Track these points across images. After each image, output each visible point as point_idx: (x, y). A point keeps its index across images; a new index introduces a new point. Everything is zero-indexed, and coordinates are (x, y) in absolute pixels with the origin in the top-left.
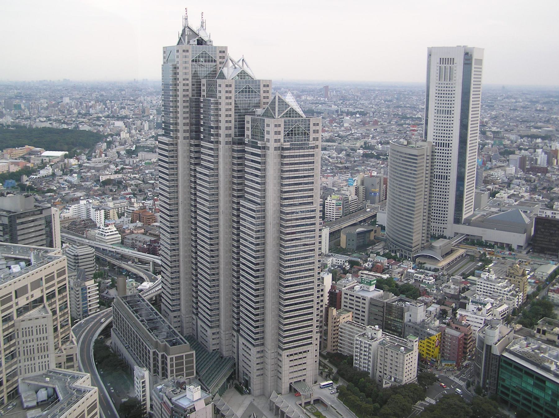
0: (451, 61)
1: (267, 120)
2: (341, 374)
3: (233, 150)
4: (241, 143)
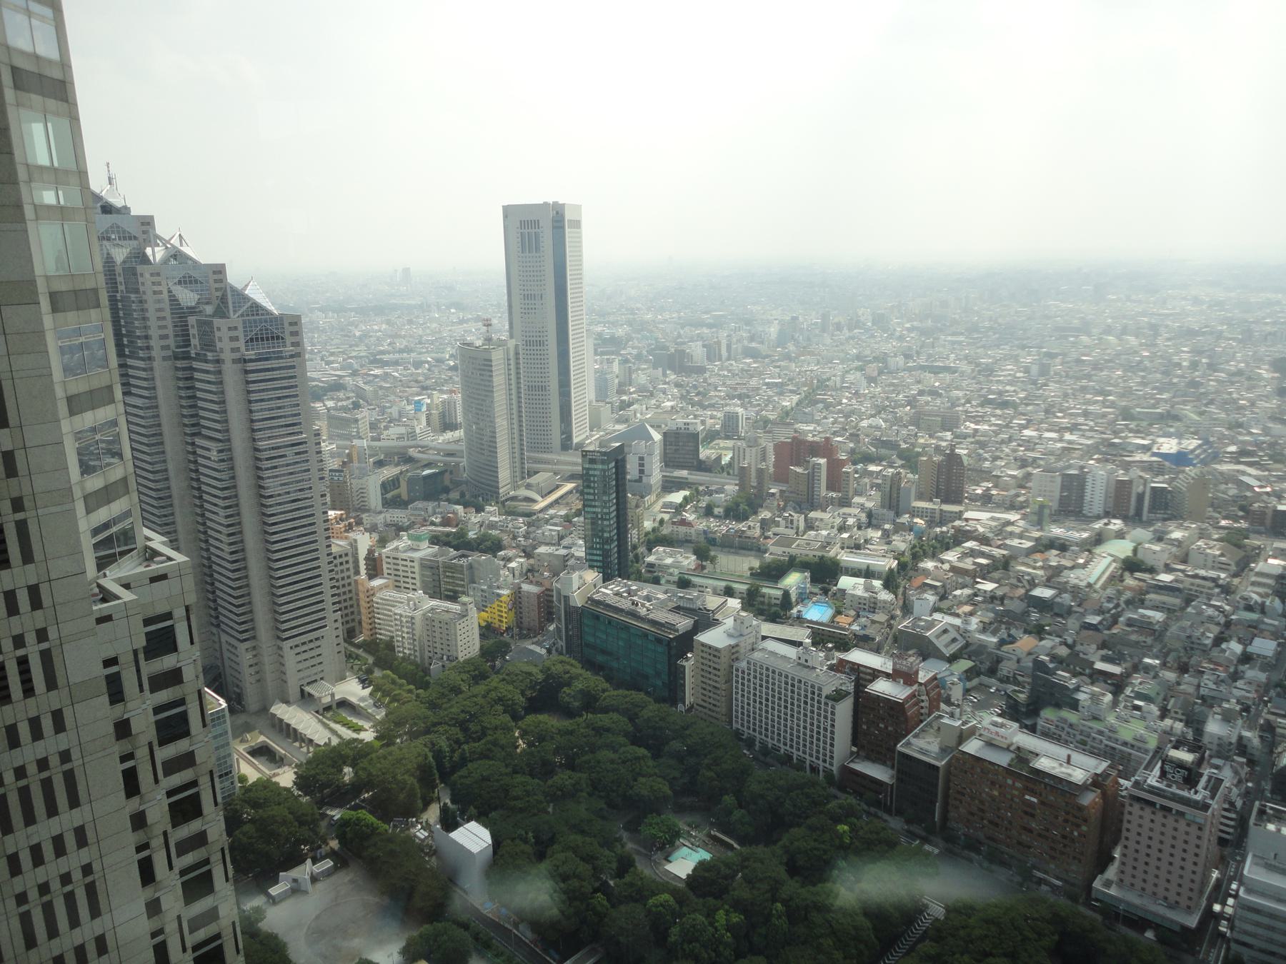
0: (536, 224)
1: (217, 322)
2: (382, 663)
3: (177, 369)
4: (186, 357)
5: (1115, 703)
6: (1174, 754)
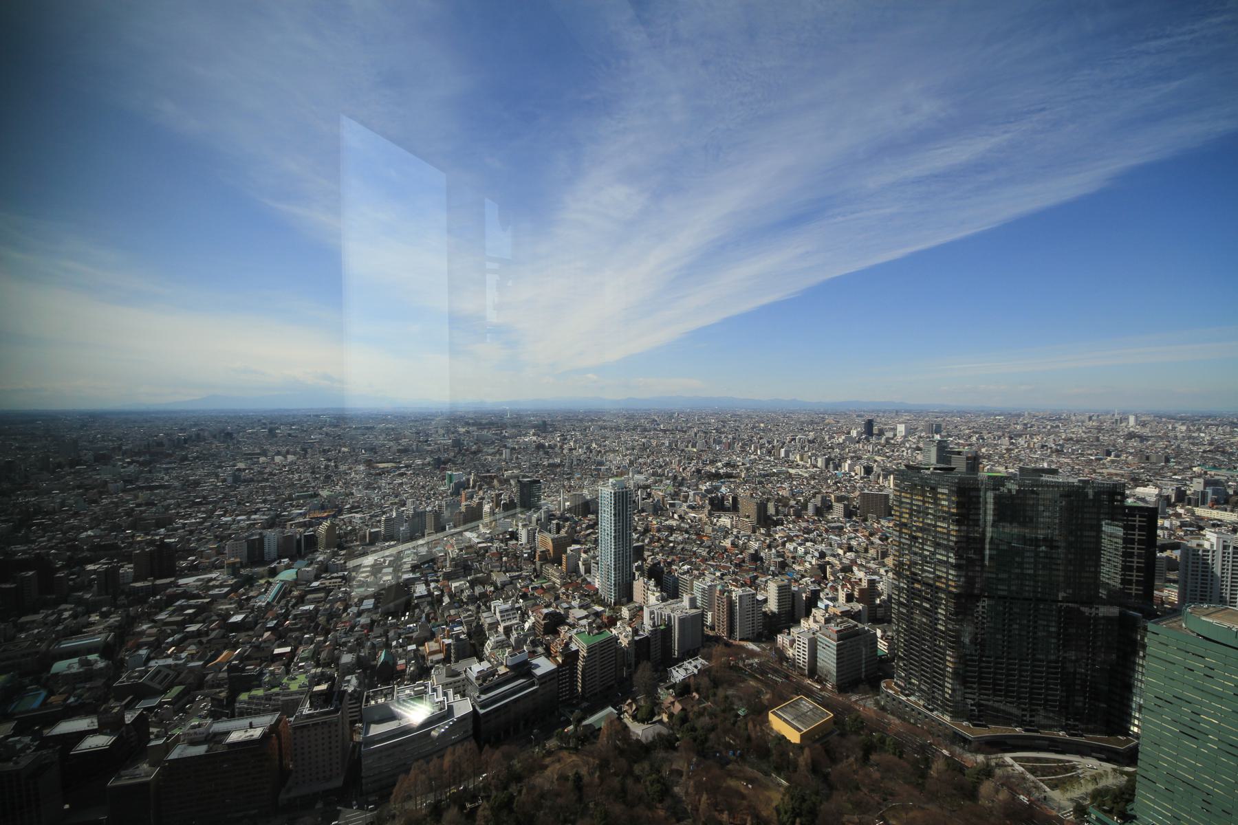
5: (288, 672)
6: (317, 688)
